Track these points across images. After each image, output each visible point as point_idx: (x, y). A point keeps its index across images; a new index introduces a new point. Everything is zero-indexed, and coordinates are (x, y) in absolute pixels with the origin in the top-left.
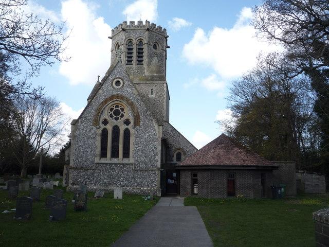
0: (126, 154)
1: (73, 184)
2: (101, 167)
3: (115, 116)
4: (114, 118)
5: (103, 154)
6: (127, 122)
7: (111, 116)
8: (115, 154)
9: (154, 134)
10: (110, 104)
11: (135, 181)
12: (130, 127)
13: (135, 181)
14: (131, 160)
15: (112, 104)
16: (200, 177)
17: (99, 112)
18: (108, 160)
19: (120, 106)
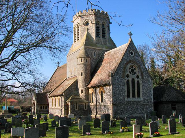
0: (139, 96)
3: (132, 73)
5: (128, 96)
6: (138, 77)
7: (130, 73)
8: (134, 96)
9: (150, 84)
10: (129, 65)
12: (139, 79)
14: (142, 99)
16: (177, 106)
18: (131, 99)
19: (133, 66)
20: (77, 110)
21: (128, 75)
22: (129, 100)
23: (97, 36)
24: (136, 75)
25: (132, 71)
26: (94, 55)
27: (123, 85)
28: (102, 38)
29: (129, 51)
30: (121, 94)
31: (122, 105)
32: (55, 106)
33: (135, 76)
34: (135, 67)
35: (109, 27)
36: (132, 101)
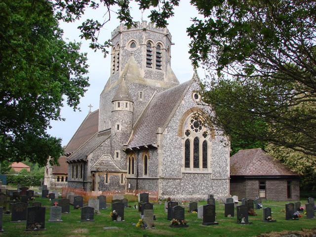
1: (163, 194)
3: (195, 128)
5: (187, 165)
6: (205, 135)
7: (192, 128)
8: (196, 165)
14: (209, 170)
16: (268, 184)
21: (188, 131)
22: (188, 171)
25: (196, 125)
27: (180, 148)
33: (200, 134)
35: (168, 50)
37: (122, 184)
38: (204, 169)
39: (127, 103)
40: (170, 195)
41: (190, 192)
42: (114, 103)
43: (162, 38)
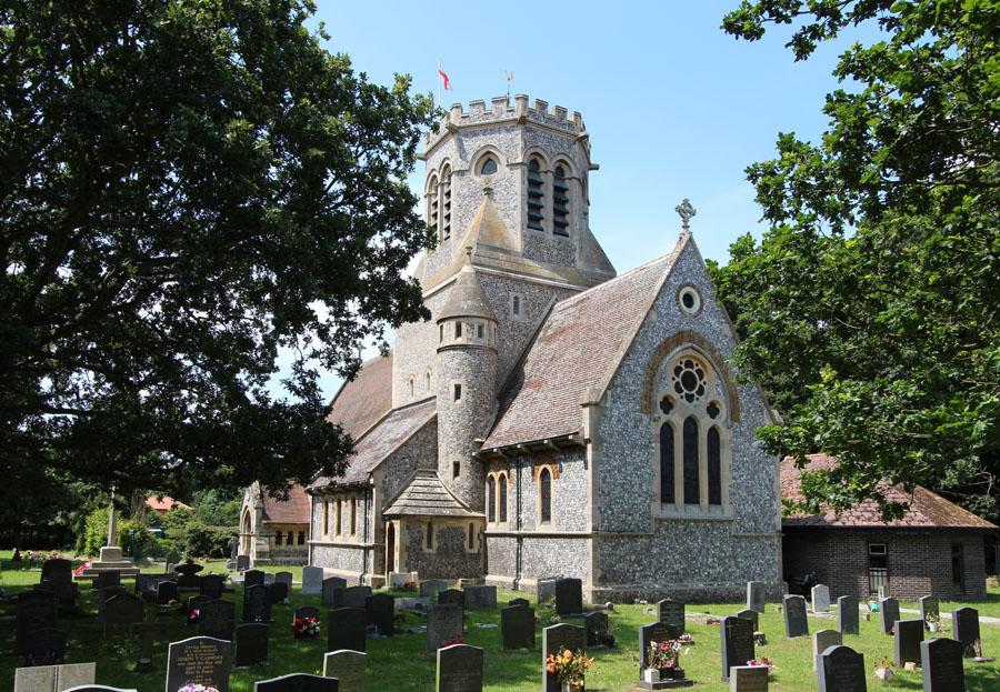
0: (715, 498)
2: (667, 530)
4: (683, 394)
5: (667, 496)
6: (713, 410)
8: (692, 497)
10: (676, 355)
11: (737, 565)
13: (737, 565)
14: (726, 511)
15: (681, 355)
17: (652, 371)
19: (695, 363)
20: (430, 551)
22: (669, 512)
23: (532, 224)
24: (704, 401)
25: (689, 381)
26: (516, 312)
28: (554, 233)
29: (679, 292)
30: (632, 486)
31: (637, 536)
32: (335, 532)
33: (698, 408)
34: (701, 362)
35: (584, 184)
36: (685, 521)
37: (471, 551)
38: (713, 507)
39: (480, 328)
40: (623, 582)
41: (678, 573)
42: (445, 324)
43: (569, 147)
